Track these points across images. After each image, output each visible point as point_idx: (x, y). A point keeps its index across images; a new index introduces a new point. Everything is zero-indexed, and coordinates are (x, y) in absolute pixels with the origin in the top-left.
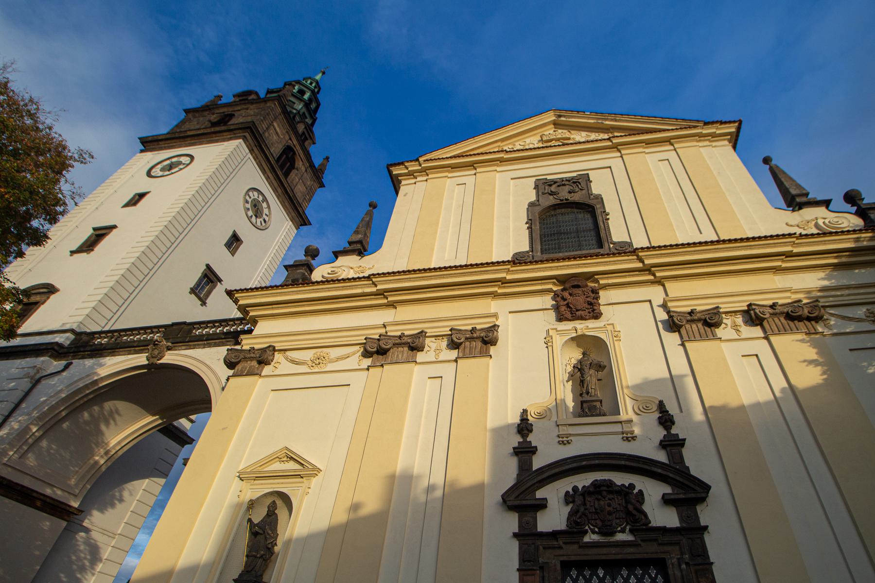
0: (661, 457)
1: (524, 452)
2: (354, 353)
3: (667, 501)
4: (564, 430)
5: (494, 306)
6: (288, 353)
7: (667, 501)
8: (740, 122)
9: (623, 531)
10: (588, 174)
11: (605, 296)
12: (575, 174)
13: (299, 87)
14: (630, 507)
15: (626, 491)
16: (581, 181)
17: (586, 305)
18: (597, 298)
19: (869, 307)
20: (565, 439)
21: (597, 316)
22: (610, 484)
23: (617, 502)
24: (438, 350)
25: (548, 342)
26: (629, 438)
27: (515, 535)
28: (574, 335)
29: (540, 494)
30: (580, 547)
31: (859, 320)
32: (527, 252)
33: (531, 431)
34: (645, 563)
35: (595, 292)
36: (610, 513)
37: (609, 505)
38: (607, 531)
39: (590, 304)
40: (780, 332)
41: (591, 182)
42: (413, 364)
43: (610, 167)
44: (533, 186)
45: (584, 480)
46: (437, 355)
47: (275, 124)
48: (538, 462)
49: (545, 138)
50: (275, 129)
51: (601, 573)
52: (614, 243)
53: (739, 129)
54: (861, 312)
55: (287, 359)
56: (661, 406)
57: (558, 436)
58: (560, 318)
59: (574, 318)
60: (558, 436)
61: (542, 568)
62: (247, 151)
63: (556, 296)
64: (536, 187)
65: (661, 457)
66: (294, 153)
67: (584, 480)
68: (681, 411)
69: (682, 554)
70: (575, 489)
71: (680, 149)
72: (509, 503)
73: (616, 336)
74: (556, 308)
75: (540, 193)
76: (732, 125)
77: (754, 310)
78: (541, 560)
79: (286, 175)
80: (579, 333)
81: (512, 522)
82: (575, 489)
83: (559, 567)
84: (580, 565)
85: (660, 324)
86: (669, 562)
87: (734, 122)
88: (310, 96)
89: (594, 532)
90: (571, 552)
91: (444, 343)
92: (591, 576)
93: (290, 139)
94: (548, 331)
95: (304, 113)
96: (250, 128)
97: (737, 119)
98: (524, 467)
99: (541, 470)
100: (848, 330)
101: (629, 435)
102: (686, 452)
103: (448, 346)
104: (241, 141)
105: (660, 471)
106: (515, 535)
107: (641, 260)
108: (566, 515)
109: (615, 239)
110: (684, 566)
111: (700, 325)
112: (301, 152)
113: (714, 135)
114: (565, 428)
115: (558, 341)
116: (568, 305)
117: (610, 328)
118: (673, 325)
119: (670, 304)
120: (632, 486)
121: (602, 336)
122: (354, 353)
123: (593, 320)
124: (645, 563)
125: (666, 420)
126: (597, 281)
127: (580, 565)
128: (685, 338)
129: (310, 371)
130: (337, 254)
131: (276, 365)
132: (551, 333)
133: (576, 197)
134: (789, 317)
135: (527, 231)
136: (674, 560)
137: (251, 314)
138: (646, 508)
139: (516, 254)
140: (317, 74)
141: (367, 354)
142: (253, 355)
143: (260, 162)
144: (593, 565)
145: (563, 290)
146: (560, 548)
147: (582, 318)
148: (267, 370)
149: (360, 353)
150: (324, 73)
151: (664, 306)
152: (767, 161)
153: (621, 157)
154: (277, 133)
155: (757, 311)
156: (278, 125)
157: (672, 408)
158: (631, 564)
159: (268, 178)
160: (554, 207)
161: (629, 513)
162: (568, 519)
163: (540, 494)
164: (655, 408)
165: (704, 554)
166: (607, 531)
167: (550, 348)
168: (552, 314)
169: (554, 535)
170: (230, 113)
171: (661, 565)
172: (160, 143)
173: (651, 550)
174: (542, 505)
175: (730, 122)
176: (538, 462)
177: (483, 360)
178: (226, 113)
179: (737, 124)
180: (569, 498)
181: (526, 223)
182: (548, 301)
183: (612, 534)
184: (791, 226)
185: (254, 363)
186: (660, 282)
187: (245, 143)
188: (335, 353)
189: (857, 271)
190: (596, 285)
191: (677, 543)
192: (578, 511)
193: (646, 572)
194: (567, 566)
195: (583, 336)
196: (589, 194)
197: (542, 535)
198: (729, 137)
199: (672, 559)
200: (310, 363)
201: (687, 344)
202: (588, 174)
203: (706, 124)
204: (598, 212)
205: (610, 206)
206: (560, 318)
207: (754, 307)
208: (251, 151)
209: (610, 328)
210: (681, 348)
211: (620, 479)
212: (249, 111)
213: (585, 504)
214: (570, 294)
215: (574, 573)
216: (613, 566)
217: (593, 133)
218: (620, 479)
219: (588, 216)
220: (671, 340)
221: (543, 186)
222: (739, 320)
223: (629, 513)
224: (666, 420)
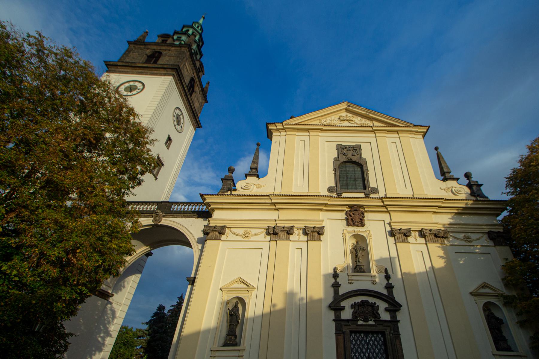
0: (385, 292)
1: (336, 286)
2: (262, 232)
3: (386, 310)
4: (351, 278)
5: (322, 215)
6: (232, 229)
7: (386, 310)
8: (429, 127)
9: (371, 320)
10: (360, 145)
11: (367, 216)
12: (354, 144)
13: (193, 30)
14: (375, 312)
15: (373, 305)
16: (357, 149)
17: (359, 220)
18: (364, 217)
19: (465, 234)
20: (351, 282)
21: (363, 225)
22: (367, 302)
23: (370, 309)
24: (299, 235)
25: (344, 236)
26: (374, 283)
27: (334, 320)
28: (354, 234)
29: (342, 304)
30: (356, 326)
31: (461, 240)
32: (334, 187)
33: (338, 277)
34: (377, 333)
35: (363, 214)
36: (367, 313)
37: (367, 310)
38: (366, 320)
39: (361, 219)
40: (433, 242)
41: (362, 150)
42: (289, 241)
43: (370, 143)
44: (336, 148)
45: (358, 299)
46: (299, 238)
47: (186, 64)
48: (342, 291)
49: (341, 119)
50: (186, 67)
51: (362, 335)
52: (371, 188)
53: (427, 130)
54: (461, 236)
55: (232, 232)
56: (386, 270)
57: (348, 280)
58: (348, 225)
59: (354, 225)
60: (348, 280)
61: (344, 333)
62: (175, 84)
63: (346, 214)
64: (337, 149)
65: (385, 292)
66: (194, 82)
67: (358, 299)
68: (393, 273)
69: (391, 330)
70: (355, 303)
71: (402, 138)
72: (332, 307)
73: (370, 236)
74: (347, 219)
75: (339, 153)
76: (425, 128)
77: (423, 231)
78: (343, 330)
79: (191, 95)
80: (356, 233)
81: (332, 315)
82: (355, 303)
83: (349, 333)
84: (356, 332)
85: (387, 232)
86: (386, 333)
87: (427, 126)
88: (199, 38)
89: (361, 320)
90: (353, 327)
91: (301, 232)
92: (359, 336)
93: (193, 73)
94: (343, 230)
95: (197, 51)
96: (176, 69)
97: (428, 125)
98: (336, 292)
99: (343, 295)
100: (456, 244)
101: (374, 282)
102: (394, 290)
103: (303, 233)
104: (171, 77)
105: (385, 298)
106: (334, 320)
107: (383, 202)
108: (351, 313)
109: (371, 186)
110: (391, 335)
111: (402, 235)
112: (198, 81)
113: (416, 132)
114: (351, 276)
115: (348, 235)
116: (352, 219)
117: (368, 232)
118: (392, 233)
119: (392, 224)
120: (375, 303)
121: (365, 236)
122: (262, 232)
123: (361, 227)
124: (377, 333)
125: (388, 277)
126: (364, 209)
127: (356, 332)
128: (397, 241)
129: (243, 240)
130: (246, 176)
131: (227, 235)
132: (345, 231)
133: (355, 159)
134: (436, 236)
135: (333, 175)
136: (388, 332)
137: (212, 207)
138: (379, 312)
139: (329, 187)
140: (200, 19)
141: (268, 234)
142: (216, 229)
143: (180, 90)
144: (360, 332)
145: (350, 211)
146: (350, 326)
147: (357, 226)
148: (223, 237)
149: (265, 233)
150: (204, 18)
151: (389, 224)
152: (436, 149)
153: (376, 137)
154: (187, 70)
155: (425, 232)
156: (188, 64)
157: (390, 273)
158: (373, 333)
159: (183, 100)
160: (345, 162)
161: (374, 314)
162: (352, 315)
163: (342, 304)
164: (384, 271)
165: (398, 331)
166: (366, 320)
167: (345, 239)
168: (345, 222)
169: (348, 321)
170: (158, 50)
171: (383, 334)
172: (119, 67)
173: (380, 328)
174: (343, 308)
175: (425, 126)
176: (342, 291)
177: (317, 243)
178: (156, 50)
179: (427, 128)
180: (353, 306)
181: (333, 170)
182: (343, 215)
183: (368, 321)
184: (442, 189)
185: (217, 233)
186: (388, 212)
187: (174, 79)
188: (254, 231)
189: (463, 216)
190: (363, 210)
191: (389, 326)
192: (356, 312)
193: (378, 336)
194: (351, 332)
195: (357, 234)
196: (361, 158)
197: (343, 320)
198: (423, 134)
199: (387, 332)
200: (243, 235)
201: (397, 244)
202: (360, 145)
203: (415, 126)
204: (365, 169)
205: (370, 166)
206: (348, 225)
207: (423, 230)
208: (176, 84)
209: (368, 232)
210: (395, 245)
211: (371, 300)
212: (170, 52)
213: (358, 309)
214: (353, 214)
215: (353, 335)
216: (366, 333)
217: (364, 119)
218: (371, 300)
219: (359, 169)
220: (391, 240)
221: (341, 149)
222: (417, 234)
223: (374, 314)
224: (388, 277)
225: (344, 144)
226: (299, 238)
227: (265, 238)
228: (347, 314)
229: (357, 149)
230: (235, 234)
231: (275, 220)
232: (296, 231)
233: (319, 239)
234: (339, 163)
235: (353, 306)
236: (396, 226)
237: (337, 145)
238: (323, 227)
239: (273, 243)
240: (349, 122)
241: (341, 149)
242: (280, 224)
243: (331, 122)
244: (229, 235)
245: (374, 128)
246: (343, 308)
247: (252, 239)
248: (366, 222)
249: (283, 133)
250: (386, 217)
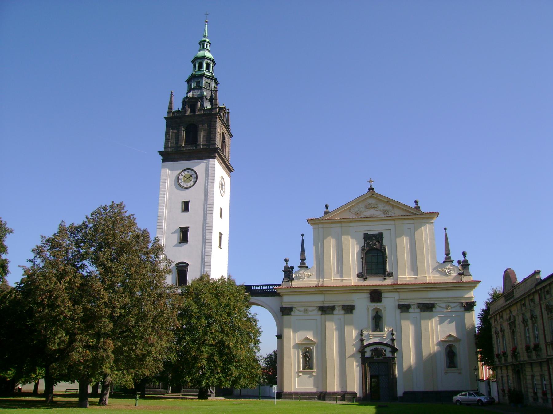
3: (390, 351)
9: (381, 357)
12: (377, 232)
16: (380, 236)
25: (368, 309)
51: (376, 364)
58: (371, 302)
65: (390, 343)
89: (376, 357)
115: (371, 309)
163: (366, 350)
168: (369, 300)
176: (365, 343)
180: (371, 350)
182: (367, 296)
188: (310, 309)
200: (304, 312)
202: (382, 233)
220: (398, 311)
221: (367, 237)
225: (369, 233)
226: (339, 312)
227: (318, 312)
228: (368, 354)
229: (380, 236)
230: (299, 311)
231: (323, 302)
232: (337, 308)
233: (351, 313)
234: (365, 251)
235: (371, 350)
236: (402, 303)
237: (365, 234)
238: (354, 305)
239: (323, 316)
240: (375, 210)
241: (367, 237)
242: (327, 304)
243: (359, 210)
244: (295, 312)
245: (394, 218)
246: (366, 352)
247: (310, 313)
248: (383, 299)
249: (320, 226)
250: (396, 295)
